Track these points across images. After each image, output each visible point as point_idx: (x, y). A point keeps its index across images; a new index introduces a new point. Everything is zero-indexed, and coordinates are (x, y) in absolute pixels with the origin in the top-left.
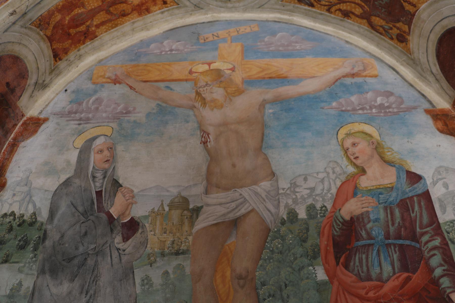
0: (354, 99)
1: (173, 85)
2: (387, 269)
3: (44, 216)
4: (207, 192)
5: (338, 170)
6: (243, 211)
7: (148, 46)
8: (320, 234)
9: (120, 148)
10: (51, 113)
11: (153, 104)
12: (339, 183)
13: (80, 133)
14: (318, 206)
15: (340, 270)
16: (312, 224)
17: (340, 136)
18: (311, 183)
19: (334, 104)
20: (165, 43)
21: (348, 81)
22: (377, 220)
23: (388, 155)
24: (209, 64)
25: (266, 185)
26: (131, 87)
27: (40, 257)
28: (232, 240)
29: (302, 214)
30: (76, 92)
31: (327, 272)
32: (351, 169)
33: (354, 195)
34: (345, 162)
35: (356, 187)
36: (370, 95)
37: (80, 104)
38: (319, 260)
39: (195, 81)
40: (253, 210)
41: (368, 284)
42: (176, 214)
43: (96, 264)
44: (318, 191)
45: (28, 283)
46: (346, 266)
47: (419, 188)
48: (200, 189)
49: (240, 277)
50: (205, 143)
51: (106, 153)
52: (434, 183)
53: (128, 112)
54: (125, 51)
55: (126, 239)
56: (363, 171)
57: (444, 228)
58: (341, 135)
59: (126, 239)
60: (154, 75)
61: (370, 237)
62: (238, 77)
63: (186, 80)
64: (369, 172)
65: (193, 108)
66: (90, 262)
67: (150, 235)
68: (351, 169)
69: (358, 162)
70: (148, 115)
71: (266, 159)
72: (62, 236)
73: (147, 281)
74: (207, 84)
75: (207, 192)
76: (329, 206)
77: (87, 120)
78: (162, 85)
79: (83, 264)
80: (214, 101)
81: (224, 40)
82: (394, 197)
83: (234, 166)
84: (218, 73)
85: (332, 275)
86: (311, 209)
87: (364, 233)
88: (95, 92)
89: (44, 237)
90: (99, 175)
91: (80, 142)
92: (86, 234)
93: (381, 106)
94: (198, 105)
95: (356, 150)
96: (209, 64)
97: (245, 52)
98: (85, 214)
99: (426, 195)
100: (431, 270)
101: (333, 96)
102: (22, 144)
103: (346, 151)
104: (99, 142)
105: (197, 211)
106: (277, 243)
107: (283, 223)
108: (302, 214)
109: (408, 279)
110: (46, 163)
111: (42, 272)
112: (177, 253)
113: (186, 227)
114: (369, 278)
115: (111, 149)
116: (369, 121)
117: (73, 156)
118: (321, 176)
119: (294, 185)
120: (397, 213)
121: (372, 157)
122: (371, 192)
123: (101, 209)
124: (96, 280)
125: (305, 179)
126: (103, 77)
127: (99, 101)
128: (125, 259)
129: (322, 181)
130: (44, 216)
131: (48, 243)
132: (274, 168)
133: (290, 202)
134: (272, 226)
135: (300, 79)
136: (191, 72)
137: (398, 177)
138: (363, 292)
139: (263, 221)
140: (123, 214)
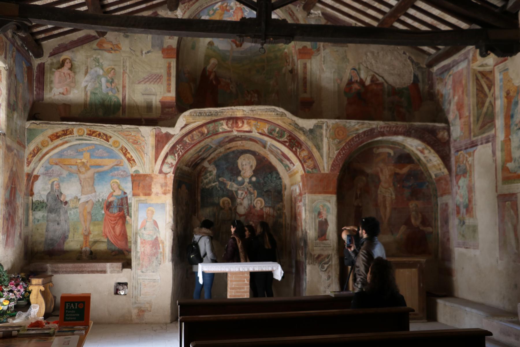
0: (116, 172)
1: (72, 166)
2: (116, 211)
3: (45, 201)
4: (81, 195)
5: (109, 191)
6: (89, 199)
7: (64, 152)
8: (104, 204)
9: (61, 184)
10: (42, 174)
11: (67, 172)
12: (109, 194)
13: (50, 180)
14: (104, 199)
15: (107, 212)
16: (103, 202)
17: (111, 183)
18: (103, 194)
19: (111, 174)
20: (69, 151)
21: (116, 167)
22: (116, 202)
23: (121, 188)
24: (81, 160)
25: (94, 194)
26: (61, 166)
27: (47, 209)
28: (87, 205)
29: (101, 200)
30: (46, 167)
31: (105, 212)
32: (112, 191)
33: (112, 196)
34: (111, 189)
35: (112, 195)
36: (120, 171)
37: (48, 171)
38: (103, 209)
39: (78, 165)
40: (91, 199)
41: (112, 214)
42: (75, 200)
43: (59, 211)
44: (104, 196)
45: (46, 215)
46: (108, 211)
47: (126, 196)
48: (80, 195)
49: (88, 212)
50: (81, 183)
51: (58, 185)
52: (129, 194)
53: (61, 174)
54: (57, 153)
55: (65, 205)
56: (114, 191)
57: (129, 204)
58: (111, 183)
59: (65, 205)
60: (66, 163)
61: (114, 205)
62: (88, 165)
63: (75, 165)
64: (116, 191)
65: (77, 174)
66: (58, 210)
67: (70, 205)
68: (112, 191)
69: (114, 189)
70: (67, 175)
71: (94, 188)
72: (51, 205)
73: (70, 213)
74: (81, 167)
75: (81, 195)
76: (106, 199)
77: (51, 176)
78: (69, 166)
79: (57, 210)
80: (82, 172)
81: (85, 151)
82: (120, 197)
83: (87, 189)
84: (83, 163)
85: (105, 212)
86: (103, 199)
87: (113, 205)
88: (51, 167)
89: (47, 205)
90: (57, 191)
91: (50, 182)
92: (56, 204)
93: (122, 175)
94: (79, 173)
95: (114, 186)
96: (81, 160)
97: (91, 156)
98: (55, 200)
99: (127, 197)
100: (124, 212)
101: (111, 171)
102: (35, 183)
103: (112, 186)
104: (55, 183)
105: (79, 199)
106: (95, 206)
107: (97, 202)
108: (101, 200)
109: (119, 214)
110: (43, 188)
111: (48, 212)
112: (76, 208)
113: (77, 203)
114: (112, 213)
115: (59, 184)
116: (118, 179)
117: (50, 186)
118: (105, 192)
119: (100, 194)
120: (120, 200)
121: (117, 188)
122: (116, 196)
123: (59, 199)
124: (60, 213)
125: (102, 193)
126: (53, 162)
127: (53, 170)
128: (65, 209)
129: (105, 193)
130: (45, 201)
131: (48, 207)
132: (96, 190)
133: (98, 198)
134: (95, 203)
135: (104, 166)
136: (76, 162)
137: (122, 193)
138: (111, 216)
139: (93, 202)
140: (64, 200)
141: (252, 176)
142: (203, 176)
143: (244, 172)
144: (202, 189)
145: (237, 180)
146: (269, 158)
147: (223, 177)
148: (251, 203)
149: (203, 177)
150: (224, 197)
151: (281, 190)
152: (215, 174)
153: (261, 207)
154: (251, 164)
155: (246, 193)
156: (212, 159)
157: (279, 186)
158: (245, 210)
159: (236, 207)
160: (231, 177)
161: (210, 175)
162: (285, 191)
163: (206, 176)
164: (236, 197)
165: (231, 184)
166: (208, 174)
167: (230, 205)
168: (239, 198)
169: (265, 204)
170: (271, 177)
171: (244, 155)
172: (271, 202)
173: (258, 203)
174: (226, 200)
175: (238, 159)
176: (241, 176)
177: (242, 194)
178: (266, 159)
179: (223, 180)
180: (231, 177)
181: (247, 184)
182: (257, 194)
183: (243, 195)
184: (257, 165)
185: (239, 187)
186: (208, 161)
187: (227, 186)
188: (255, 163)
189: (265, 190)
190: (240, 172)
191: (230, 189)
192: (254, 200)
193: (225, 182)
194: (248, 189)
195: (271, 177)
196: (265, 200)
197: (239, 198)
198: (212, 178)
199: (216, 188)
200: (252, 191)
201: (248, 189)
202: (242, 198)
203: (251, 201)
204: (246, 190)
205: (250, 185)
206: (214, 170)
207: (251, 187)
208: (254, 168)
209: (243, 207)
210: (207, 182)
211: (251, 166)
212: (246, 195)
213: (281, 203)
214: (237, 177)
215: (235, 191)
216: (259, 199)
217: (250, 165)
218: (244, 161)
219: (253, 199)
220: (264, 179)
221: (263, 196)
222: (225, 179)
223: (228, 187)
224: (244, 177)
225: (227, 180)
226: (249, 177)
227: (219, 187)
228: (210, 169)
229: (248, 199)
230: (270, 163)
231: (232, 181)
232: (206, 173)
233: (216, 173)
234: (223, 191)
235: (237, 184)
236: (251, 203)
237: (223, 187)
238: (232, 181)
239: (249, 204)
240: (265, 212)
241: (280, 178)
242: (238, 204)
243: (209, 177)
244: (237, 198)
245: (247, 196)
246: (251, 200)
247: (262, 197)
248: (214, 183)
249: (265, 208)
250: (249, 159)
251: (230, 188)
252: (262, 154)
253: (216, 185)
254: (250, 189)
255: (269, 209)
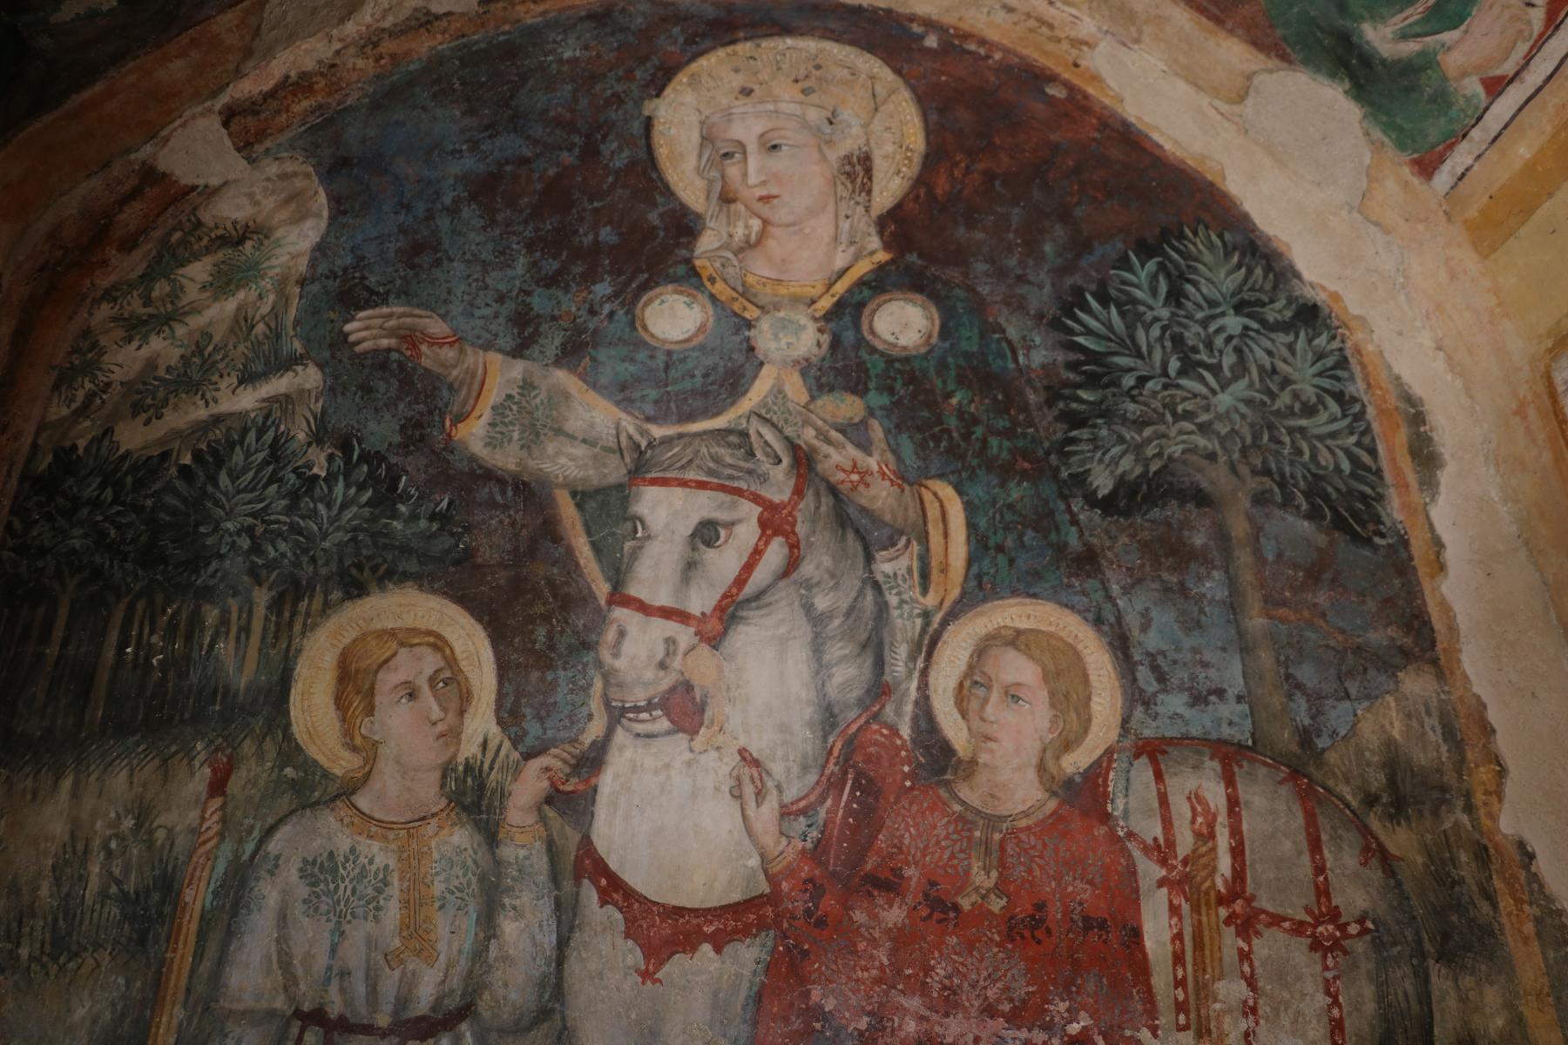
141: (878, 284)
142: (109, 295)
143: (745, 226)
144: (44, 463)
145: (634, 339)
146: (1095, 78)
147: (406, 294)
148: (880, 690)
149: (105, 310)
150: (390, 576)
151: (1366, 471)
152: (302, 266)
153: (1076, 761)
154: (850, 143)
155: (774, 523)
156: (299, 85)
157: (1318, 424)
158: (764, 817)
159: (592, 761)
160: (539, 302)
161: (224, 283)
162: (1429, 484)
163: (160, 288)
164: (602, 589)
165: (527, 385)
166: (198, 271)
167: (481, 723)
168: (644, 608)
169: (1136, 697)
170: (1176, 297)
171: (744, 48)
172: (1233, 675)
173: (1013, 695)
174: (406, 638)
175: (660, 82)
176: (692, 278)
177: (707, 533)
178: (1055, 91)
179: (411, 338)
180: (539, 302)
181: (796, 389)
182: (980, 543)
183: (724, 562)
184: (935, 157)
185: (658, 432)
186: (229, 116)
187: (460, 418)
188: (917, 140)
189: (1103, 483)
190: (685, 226)
191: (507, 459)
192: (928, 646)
193: (429, 357)
194: (803, 462)
195: (1176, 297)
196: (1121, 645)
197: (644, 608)
198: (242, 322)
199: (277, 451)
200: (881, 496)
201: (803, 462)
202: (700, 601)
203: (879, 664)
204: (779, 485)
205: (849, 407)
206: (298, 218)
207: (855, 432)
208: (889, 188)
209: (718, 767)
210: (151, 365)
211: (859, 169)
212: (776, 552)
213: (1416, 684)
214: (631, 295)
215: (581, 497)
216: (1013, 613)
217: (834, 155)
218: (742, 106)
219: (904, 626)
220: (1058, 323)
221: (1088, 562)
222: (437, 327)
223: (474, 434)
224: (746, 293)
225: (458, 340)
226: (826, 303)
227: (317, 438)
228: (230, 210)
229: (817, 620)
230: (1129, 138)
231: (552, 342)
232: (169, 259)
233: (321, 249)
234: (387, 495)
235: (623, 393)
236: (880, 690)
237: (381, 431)
238: (552, 342)
239: (828, 717)
240: (1162, 852)
241: (1310, 315)
242: (617, 715)
243: (195, 310)
244: (619, 597)
245: (791, 565)
246: (875, 647)
247: (1057, 596)
248: (248, 378)
249: (1142, 772)
250: (809, 83)
251: (491, 443)
252: (993, 35)
253: (285, 402)
254: (837, 458)
255: (1216, 795)
